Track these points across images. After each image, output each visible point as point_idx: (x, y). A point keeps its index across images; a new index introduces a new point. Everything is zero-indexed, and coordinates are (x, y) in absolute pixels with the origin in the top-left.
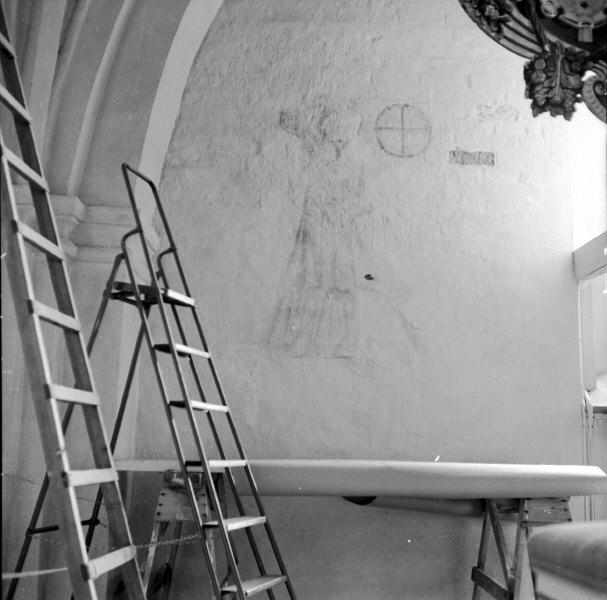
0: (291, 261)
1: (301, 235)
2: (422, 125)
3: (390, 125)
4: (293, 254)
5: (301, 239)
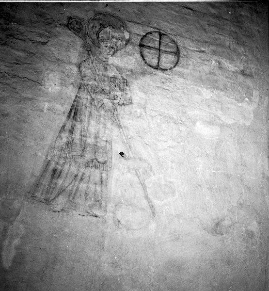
0: (61, 132)
1: (73, 111)
2: (172, 50)
3: (149, 45)
4: (64, 126)
5: (72, 114)
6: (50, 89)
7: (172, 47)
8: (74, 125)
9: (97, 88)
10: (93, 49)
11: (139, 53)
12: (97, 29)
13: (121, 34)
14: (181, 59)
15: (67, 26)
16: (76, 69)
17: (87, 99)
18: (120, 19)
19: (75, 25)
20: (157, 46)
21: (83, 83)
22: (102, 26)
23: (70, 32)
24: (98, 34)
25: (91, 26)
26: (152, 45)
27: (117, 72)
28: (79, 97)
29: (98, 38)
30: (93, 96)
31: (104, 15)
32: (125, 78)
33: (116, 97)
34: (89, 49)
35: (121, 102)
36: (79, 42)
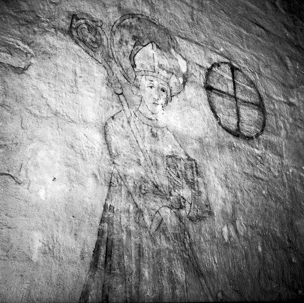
1: (103, 249)
2: (253, 100)
6: (42, 194)
7: (251, 93)
8: (110, 288)
9: (145, 182)
10: (127, 92)
11: (207, 102)
12: (130, 48)
13: (173, 62)
14: (268, 116)
15: (69, 32)
16: (98, 138)
17: (128, 211)
18: (167, 32)
19: (86, 32)
20: (231, 91)
21: (115, 171)
22: (138, 41)
23: (76, 47)
24: (132, 58)
25: (118, 39)
26: (224, 90)
27: (176, 143)
28: (111, 208)
29: (134, 66)
30: (140, 202)
31: (139, 18)
32: (192, 156)
33: (182, 200)
34: (119, 91)
35: (193, 213)
36: (99, 73)
